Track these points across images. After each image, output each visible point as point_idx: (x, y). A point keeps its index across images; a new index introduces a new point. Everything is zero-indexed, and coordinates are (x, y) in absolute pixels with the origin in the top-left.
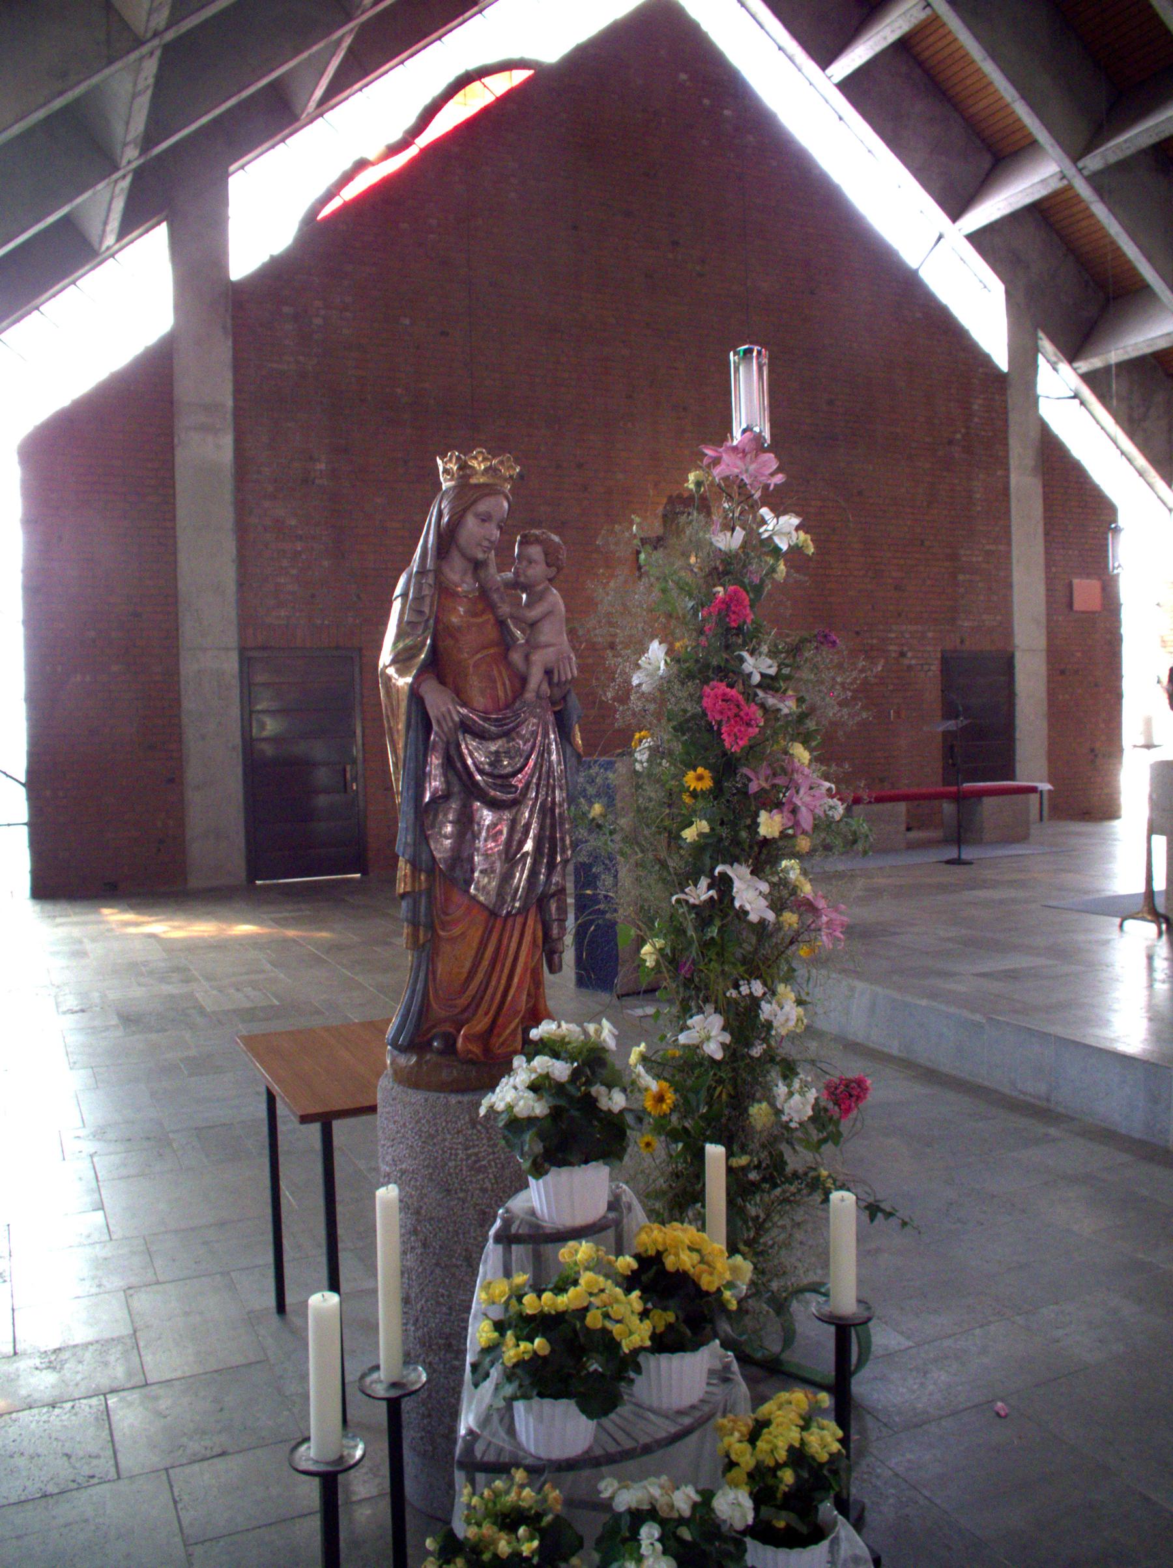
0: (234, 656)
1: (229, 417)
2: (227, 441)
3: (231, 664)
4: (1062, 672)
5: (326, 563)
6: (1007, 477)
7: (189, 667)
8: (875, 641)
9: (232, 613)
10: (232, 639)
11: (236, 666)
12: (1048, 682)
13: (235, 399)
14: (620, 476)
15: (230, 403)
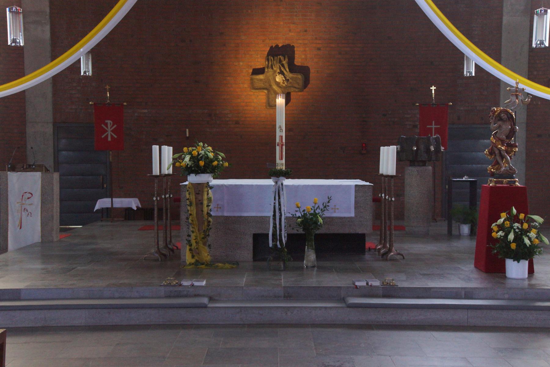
0: (51, 126)
1: (48, 17)
2: (48, 28)
3: (49, 129)
4: (539, 136)
5: (94, 84)
6: (501, 18)
7: (30, 130)
8: (396, 120)
9: (50, 108)
10: (49, 117)
11: (52, 130)
12: (527, 142)
13: (51, 9)
14: (243, 37)
15: (48, 10)
